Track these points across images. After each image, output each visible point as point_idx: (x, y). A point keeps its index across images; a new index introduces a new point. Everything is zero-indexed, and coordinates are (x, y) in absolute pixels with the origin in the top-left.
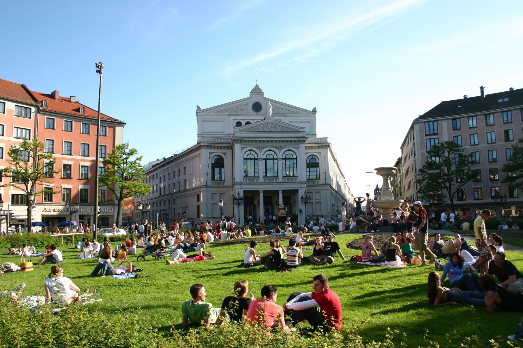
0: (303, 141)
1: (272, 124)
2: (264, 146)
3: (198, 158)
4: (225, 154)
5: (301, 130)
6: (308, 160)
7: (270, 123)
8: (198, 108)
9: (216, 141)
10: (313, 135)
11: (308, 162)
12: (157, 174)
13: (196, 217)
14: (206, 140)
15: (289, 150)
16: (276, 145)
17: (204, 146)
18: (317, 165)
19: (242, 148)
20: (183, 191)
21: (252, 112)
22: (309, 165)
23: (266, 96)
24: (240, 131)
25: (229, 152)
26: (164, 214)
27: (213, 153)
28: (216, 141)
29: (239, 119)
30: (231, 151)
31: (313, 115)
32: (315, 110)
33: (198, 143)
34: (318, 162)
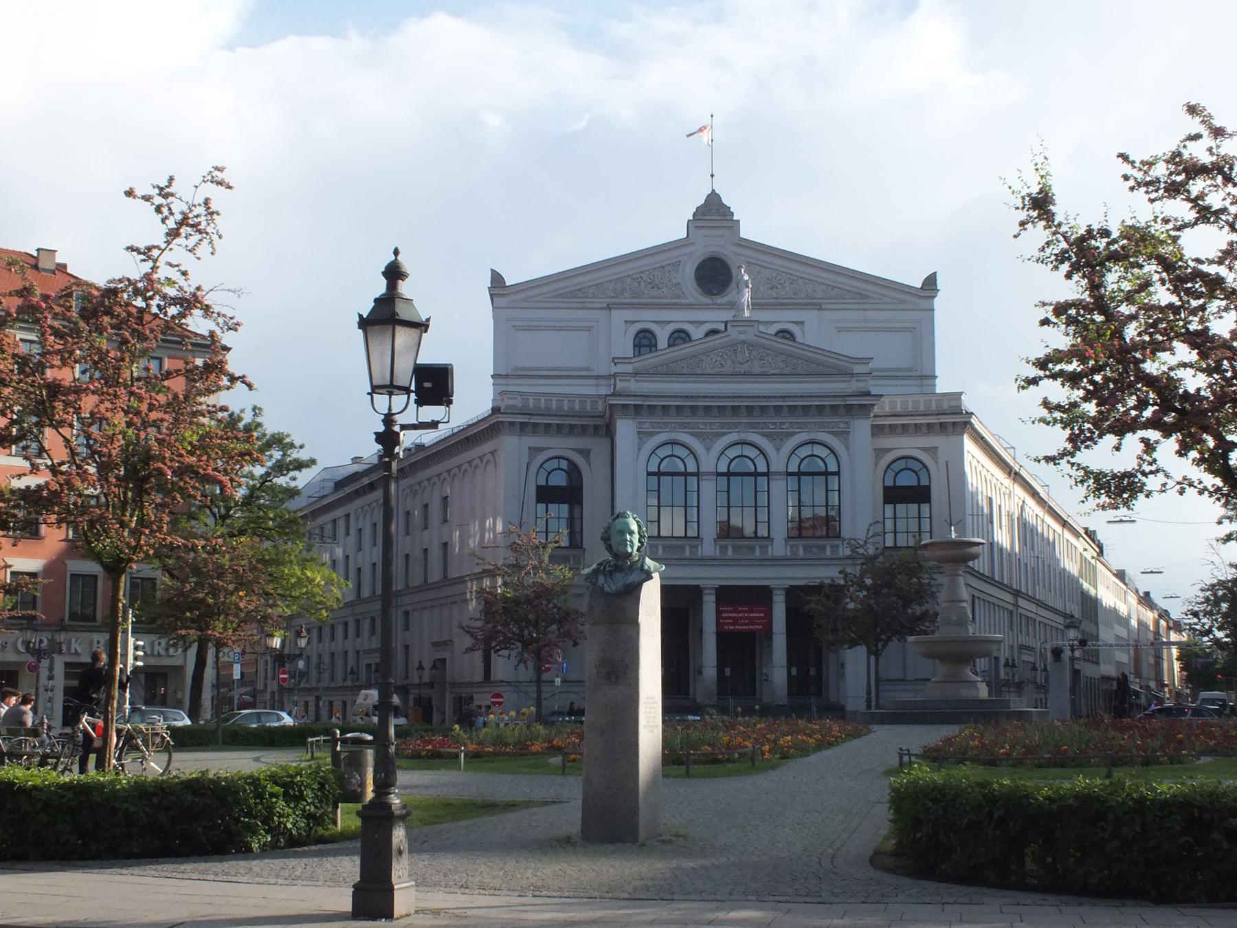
0: (865, 409)
1: (751, 345)
2: (722, 425)
3: (490, 467)
4: (585, 453)
5: (857, 369)
6: (891, 474)
7: (743, 342)
8: (497, 279)
9: (554, 405)
10: (922, 377)
11: (889, 483)
12: (348, 516)
13: (479, 678)
14: (518, 402)
15: (813, 442)
16: (766, 425)
17: (512, 424)
18: (920, 494)
19: (643, 435)
20: (418, 590)
21: (692, 291)
22: (893, 495)
23: (744, 234)
24: (636, 374)
25: (598, 446)
26: (369, 666)
27: (540, 450)
28: (554, 405)
29: (646, 318)
30: (605, 442)
31: (923, 304)
32: (931, 283)
33: (495, 410)
34: (924, 482)
